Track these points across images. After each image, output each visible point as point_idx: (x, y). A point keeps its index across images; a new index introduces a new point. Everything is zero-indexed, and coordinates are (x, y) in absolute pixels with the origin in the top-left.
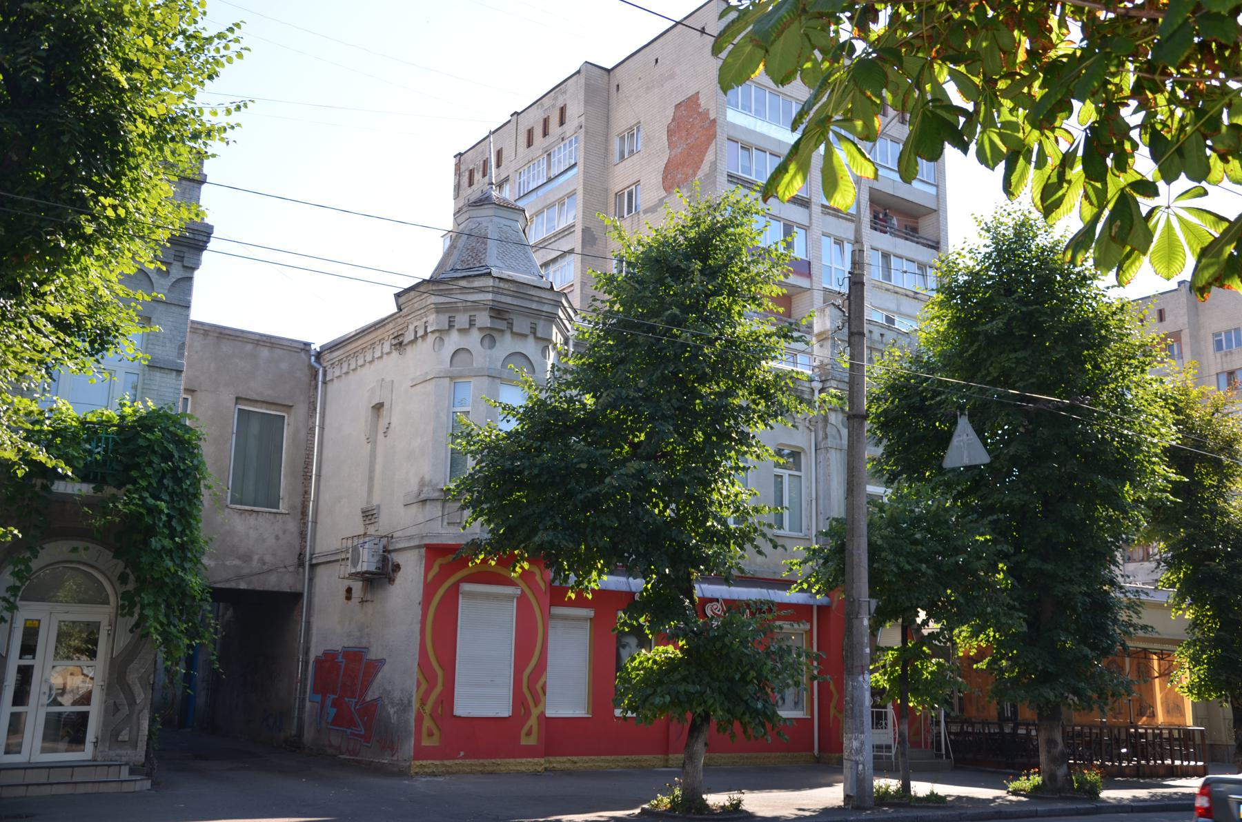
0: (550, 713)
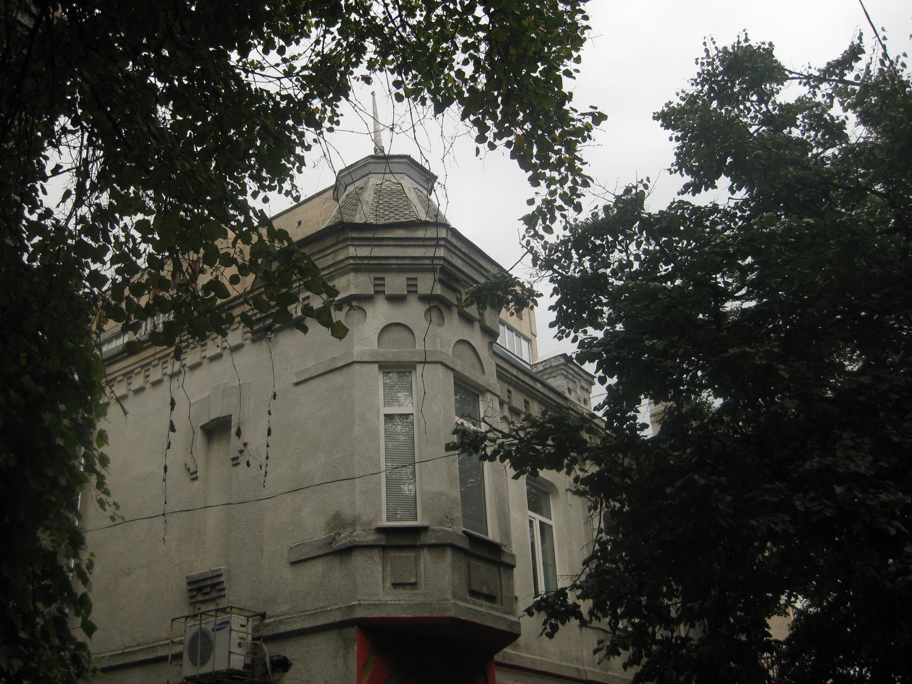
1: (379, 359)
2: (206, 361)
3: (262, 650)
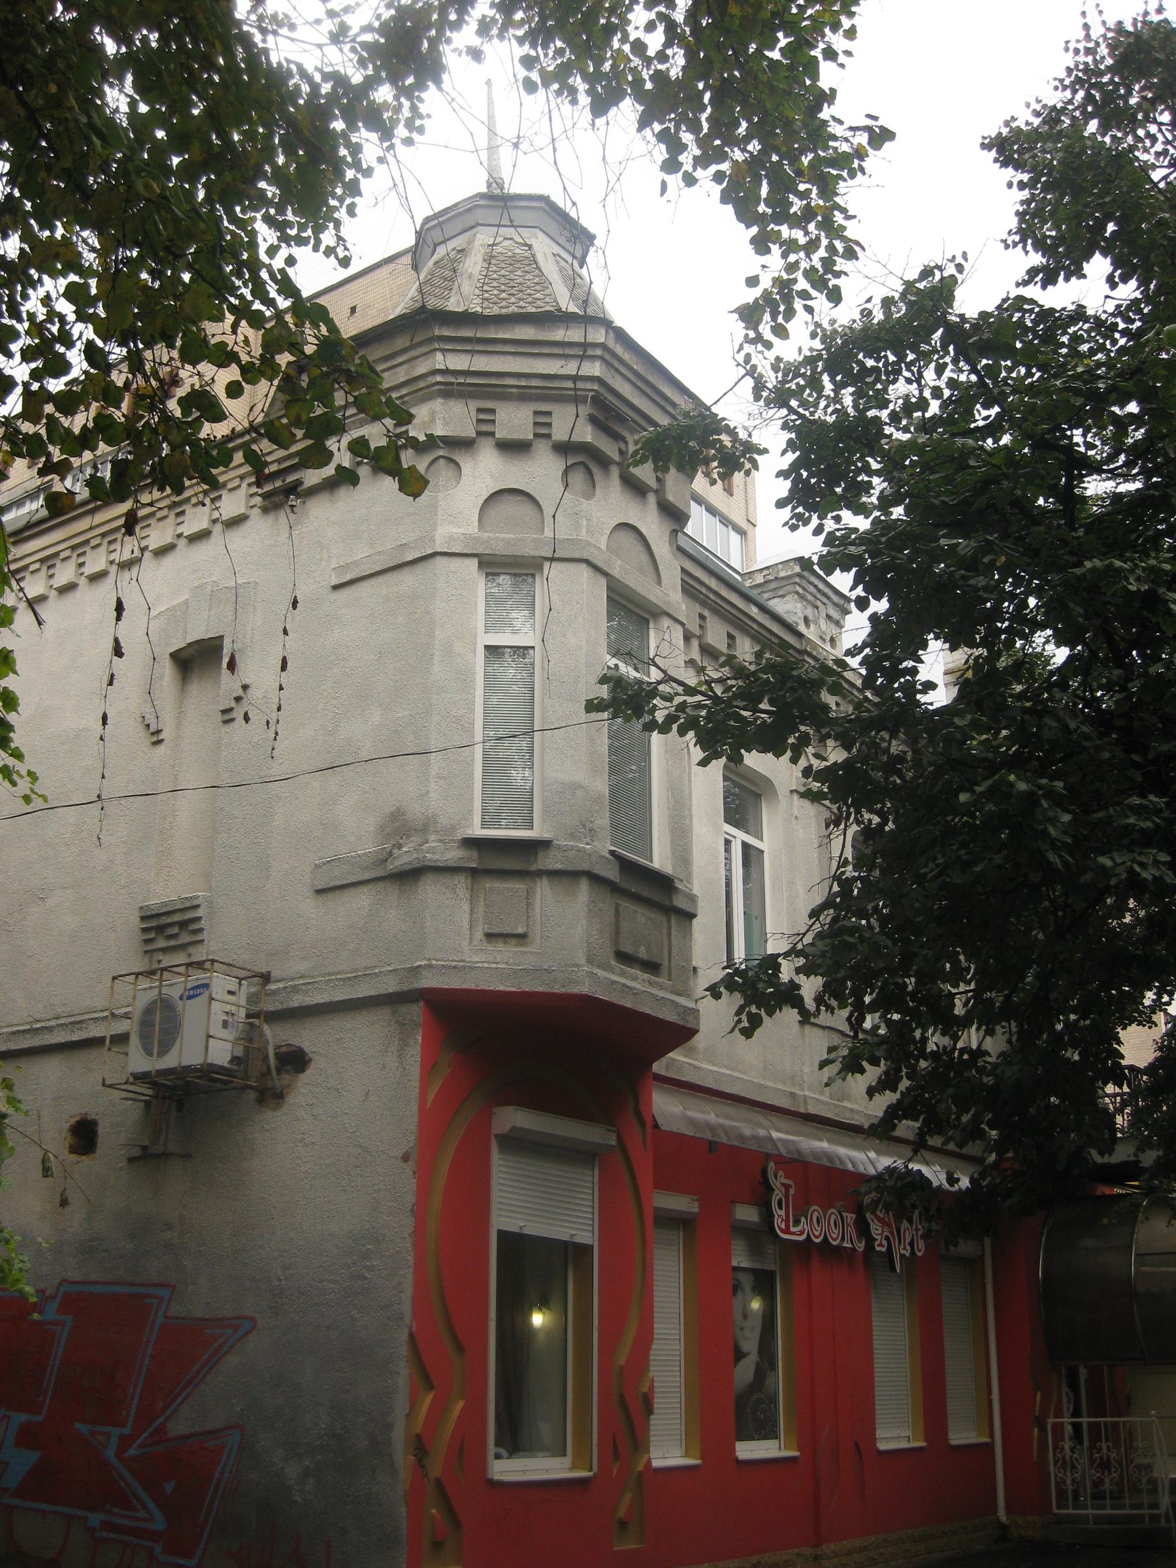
0: (656, 1463)
1: (480, 550)
2: (182, 543)
3: (262, 1034)
